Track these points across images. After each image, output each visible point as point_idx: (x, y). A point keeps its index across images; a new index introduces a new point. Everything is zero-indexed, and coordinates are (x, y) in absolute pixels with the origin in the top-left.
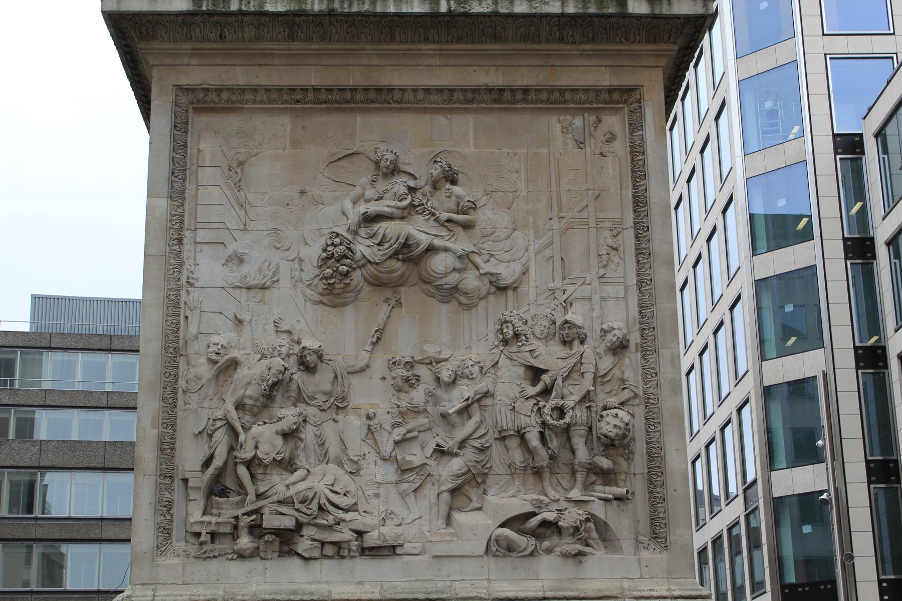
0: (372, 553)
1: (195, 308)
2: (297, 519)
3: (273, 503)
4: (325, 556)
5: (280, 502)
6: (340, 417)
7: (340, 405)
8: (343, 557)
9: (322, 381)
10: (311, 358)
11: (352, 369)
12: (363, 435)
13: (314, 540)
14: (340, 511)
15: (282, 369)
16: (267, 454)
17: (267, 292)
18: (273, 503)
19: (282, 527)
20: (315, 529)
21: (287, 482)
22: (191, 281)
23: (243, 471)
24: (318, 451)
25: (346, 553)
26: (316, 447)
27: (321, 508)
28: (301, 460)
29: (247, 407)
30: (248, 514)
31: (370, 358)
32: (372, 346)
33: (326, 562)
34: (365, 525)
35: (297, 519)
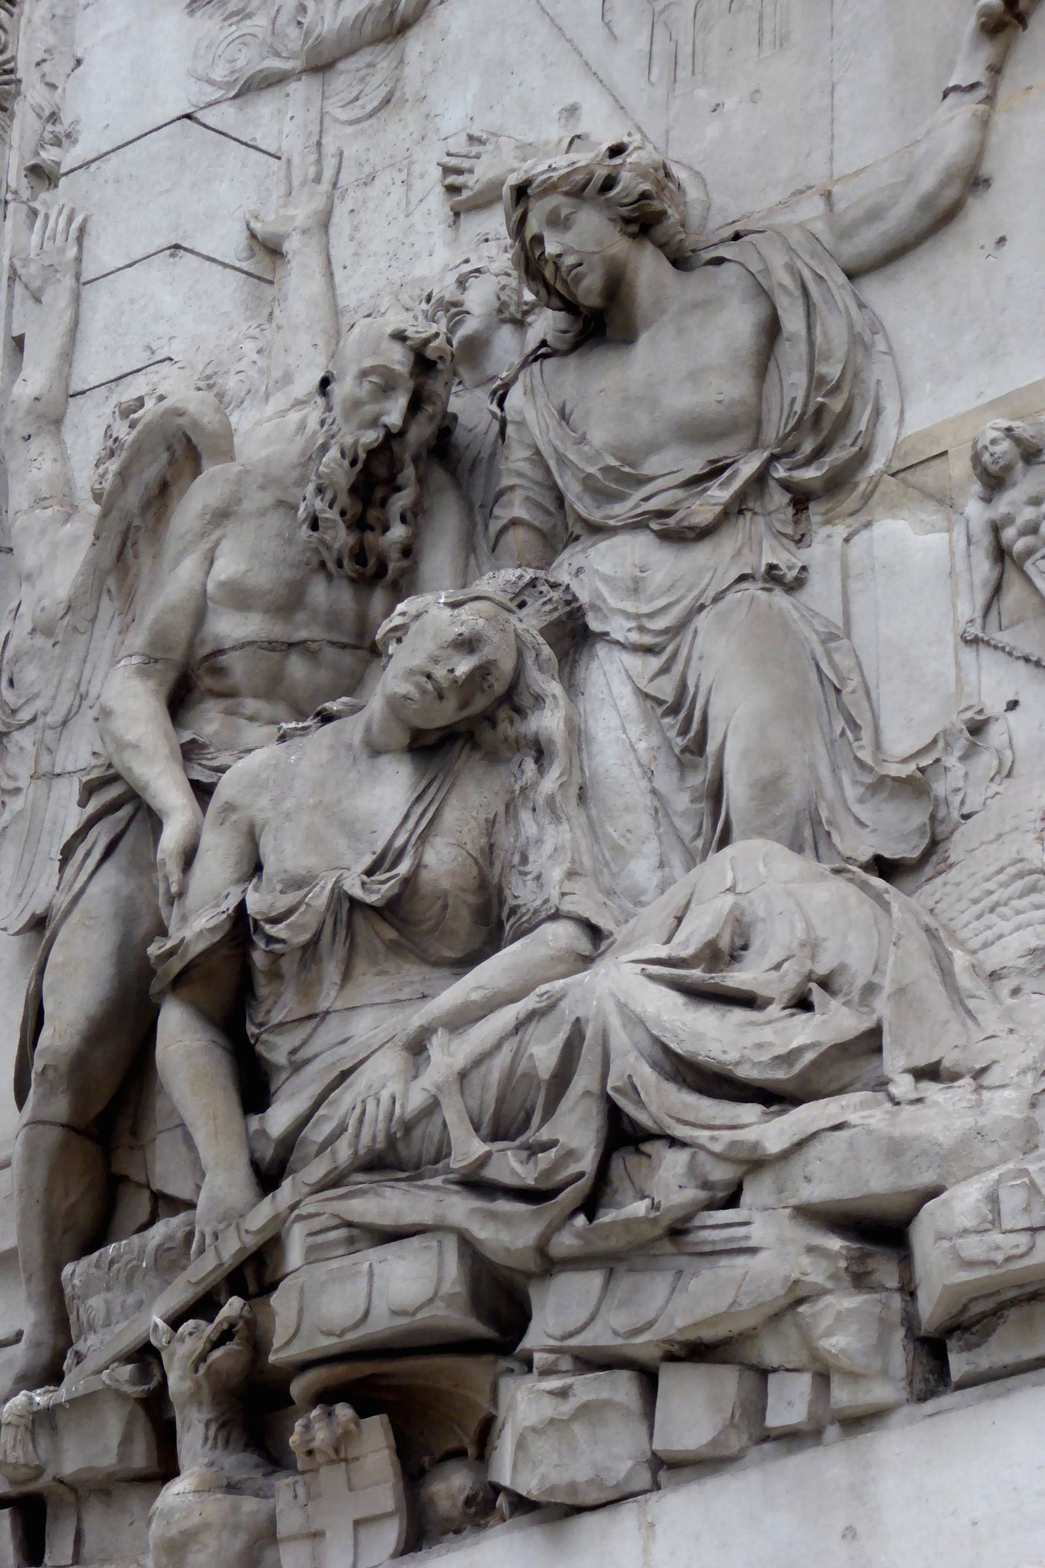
0: (996, 1353)
1: (51, 270)
2: (469, 1249)
3: (334, 1181)
4: (667, 1468)
5: (386, 1162)
6: (825, 543)
7: (810, 473)
8: (791, 1438)
9: (688, 357)
10: (584, 239)
11: (869, 240)
12: (968, 608)
13: (594, 1362)
14: (750, 1112)
15: (398, 358)
16: (299, 883)
17: (414, 44)
18: (334, 1181)
19: (381, 1324)
20: (593, 1280)
21: (418, 1017)
22: (49, 155)
23: (181, 1039)
24: (681, 801)
25: (789, 1403)
26: (666, 780)
27: (624, 1135)
28: (549, 861)
29: (237, 665)
30: (204, 1306)
31: (985, 124)
32: (986, 53)
33: (679, 1506)
34: (895, 1149)
35: (468, 1246)
